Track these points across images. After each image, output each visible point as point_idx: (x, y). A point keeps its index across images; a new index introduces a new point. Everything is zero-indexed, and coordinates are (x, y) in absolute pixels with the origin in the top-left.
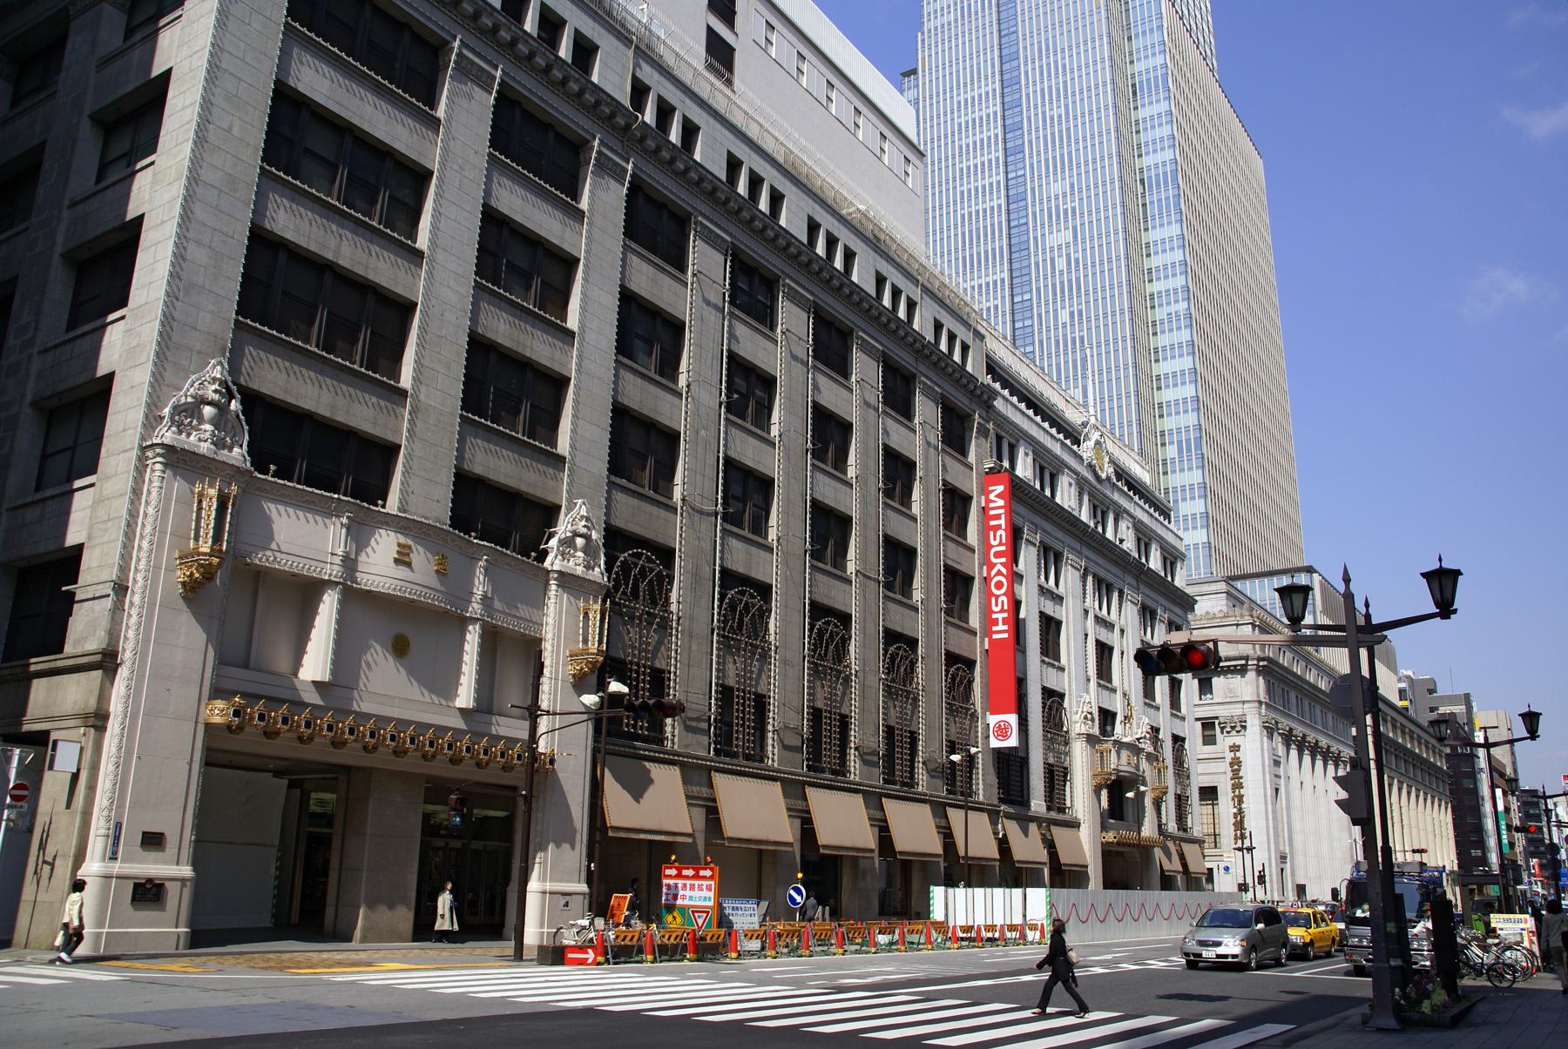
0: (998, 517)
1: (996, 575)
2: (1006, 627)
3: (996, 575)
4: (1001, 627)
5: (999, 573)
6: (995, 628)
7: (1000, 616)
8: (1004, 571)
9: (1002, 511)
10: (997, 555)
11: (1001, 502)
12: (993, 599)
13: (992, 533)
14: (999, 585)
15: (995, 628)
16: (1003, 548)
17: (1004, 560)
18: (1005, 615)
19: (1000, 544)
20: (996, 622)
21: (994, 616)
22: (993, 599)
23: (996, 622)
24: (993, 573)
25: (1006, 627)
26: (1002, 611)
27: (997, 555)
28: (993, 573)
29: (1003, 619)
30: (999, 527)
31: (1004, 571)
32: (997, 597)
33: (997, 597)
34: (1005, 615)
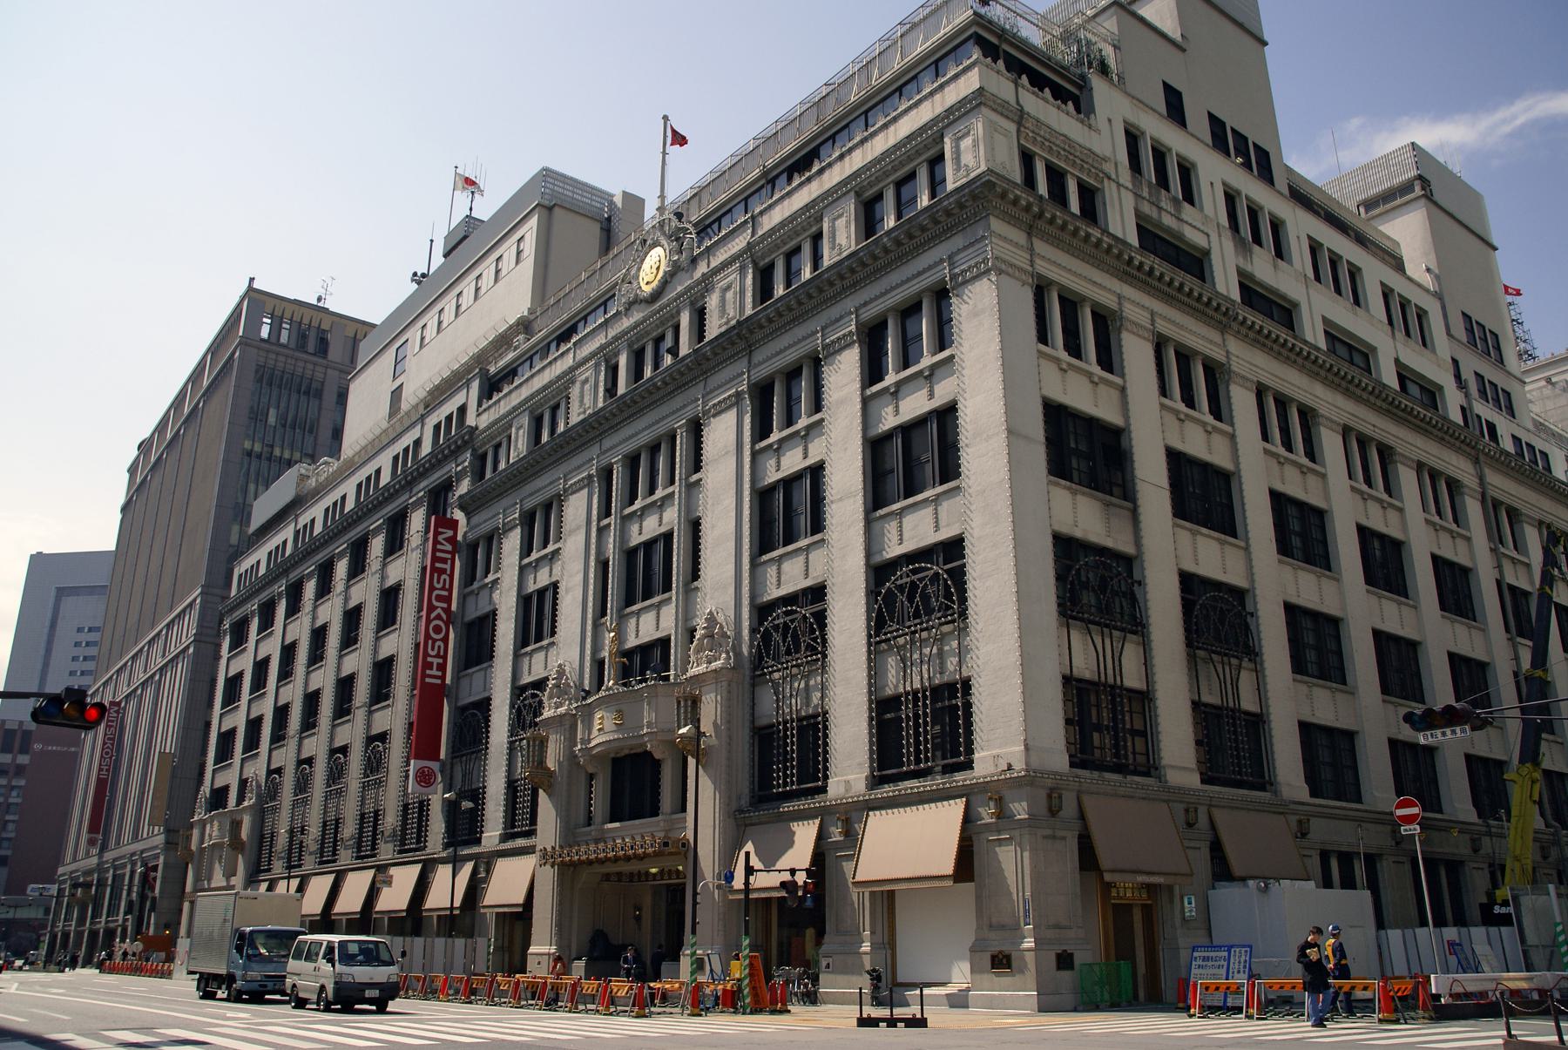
1: (435, 619)
2: (440, 673)
3: (435, 619)
4: (434, 672)
5: (438, 617)
6: (428, 672)
7: (436, 661)
8: (444, 617)
9: (449, 556)
12: (430, 642)
15: (428, 672)
17: (445, 605)
18: (441, 661)
19: (443, 588)
20: (430, 666)
21: (429, 659)
22: (430, 642)
23: (430, 666)
24: (433, 616)
25: (440, 673)
26: (438, 656)
27: (439, 598)
28: (433, 616)
29: (438, 664)
30: (443, 571)
31: (444, 617)
32: (434, 641)
33: (434, 641)
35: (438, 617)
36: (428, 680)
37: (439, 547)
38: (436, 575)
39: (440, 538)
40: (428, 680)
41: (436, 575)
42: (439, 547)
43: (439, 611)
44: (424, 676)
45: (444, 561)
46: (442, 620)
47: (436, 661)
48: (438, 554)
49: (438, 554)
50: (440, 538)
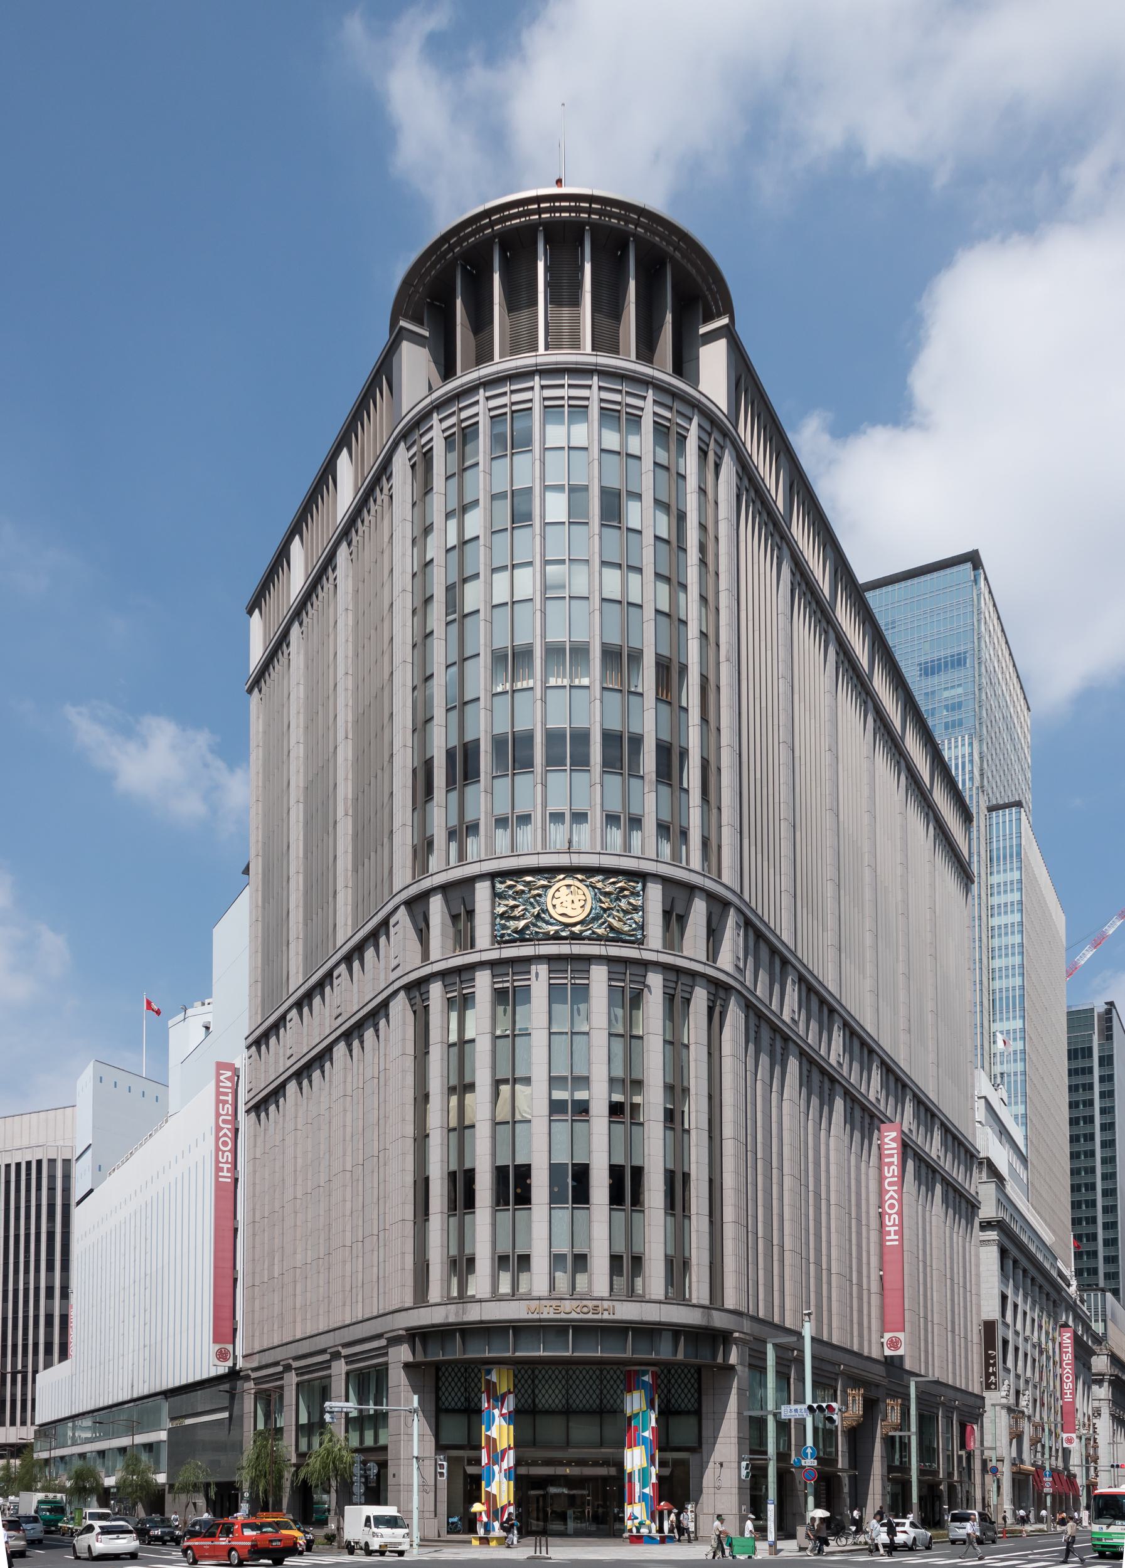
0: (226, 1094)
2: (229, 1175)
4: (225, 1174)
5: (225, 1135)
6: (220, 1174)
7: (226, 1166)
8: (230, 1135)
10: (224, 1121)
11: (229, 1084)
12: (220, 1153)
13: (886, 1168)
14: (225, 1144)
15: (220, 1174)
16: (896, 1179)
18: (229, 1166)
19: (227, 1114)
20: (222, 1170)
21: (220, 1165)
22: (220, 1153)
23: (222, 1170)
24: (221, 1134)
26: (227, 1162)
27: (224, 1121)
28: (221, 1134)
30: (226, 1102)
31: (230, 1135)
32: (224, 1152)
34: (229, 1166)
35: (225, 1135)
36: (221, 1179)
37: (221, 1084)
38: (221, 1105)
39: (222, 1078)
40: (221, 1179)
41: (221, 1105)
42: (221, 1084)
43: (225, 1131)
44: (217, 1177)
45: (226, 1094)
46: (228, 1137)
47: (226, 1166)
48: (221, 1090)
49: (221, 1090)
50: (222, 1078)
